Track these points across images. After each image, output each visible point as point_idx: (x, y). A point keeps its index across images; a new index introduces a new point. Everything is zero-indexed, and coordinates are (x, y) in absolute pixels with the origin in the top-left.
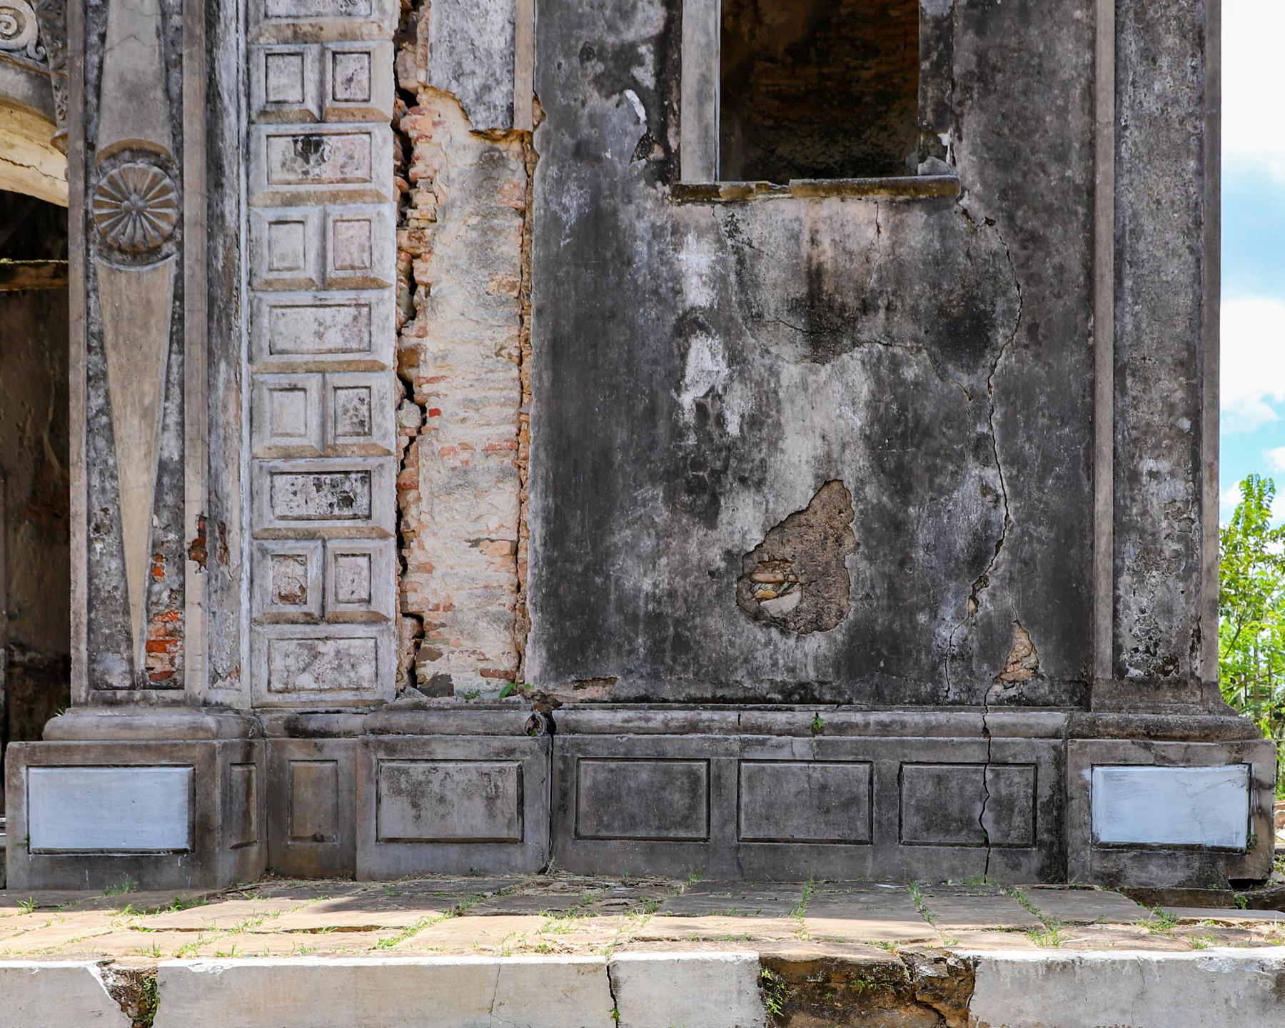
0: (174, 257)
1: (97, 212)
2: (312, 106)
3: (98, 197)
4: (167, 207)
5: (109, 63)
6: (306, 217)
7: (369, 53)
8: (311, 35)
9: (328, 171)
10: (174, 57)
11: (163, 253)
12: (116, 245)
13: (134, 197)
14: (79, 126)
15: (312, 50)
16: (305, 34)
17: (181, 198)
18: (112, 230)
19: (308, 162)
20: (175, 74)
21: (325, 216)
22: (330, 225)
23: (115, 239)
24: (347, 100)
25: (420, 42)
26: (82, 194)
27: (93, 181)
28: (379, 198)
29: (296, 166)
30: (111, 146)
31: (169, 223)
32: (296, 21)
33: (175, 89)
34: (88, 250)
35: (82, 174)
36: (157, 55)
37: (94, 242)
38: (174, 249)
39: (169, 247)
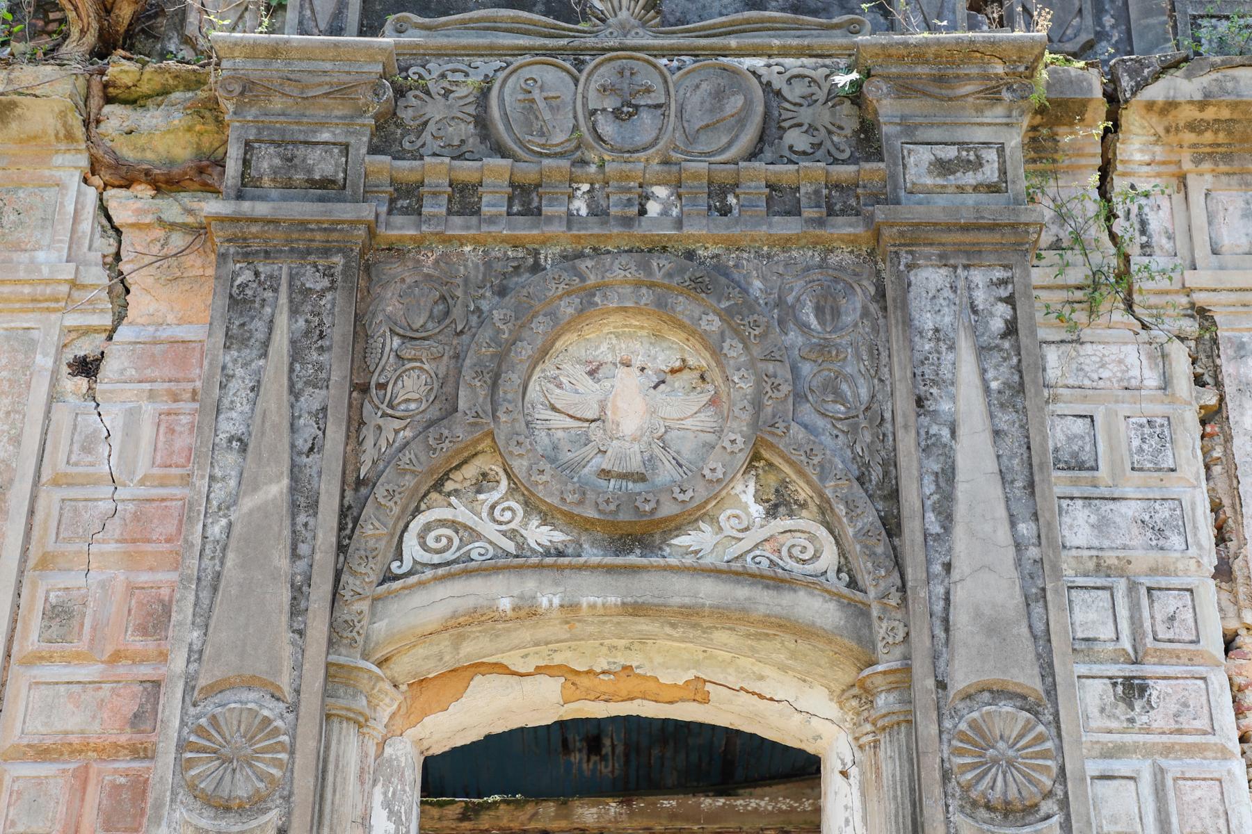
0: (1055, 819)
1: (960, 761)
2: (1126, 644)
3: (955, 743)
4: (1045, 758)
5: (958, 596)
6: (1138, 772)
7: (1191, 591)
8: (1116, 568)
9: (1158, 719)
10: (1034, 590)
11: (1042, 813)
12: (982, 802)
13: (1001, 745)
14: (928, 661)
15: (1121, 585)
16: (1109, 567)
17: (1060, 748)
18: (977, 783)
19: (1133, 710)
20: (1037, 609)
21: (1159, 773)
22: (1169, 782)
23: (984, 794)
24: (1170, 641)
25: (1240, 580)
26: (937, 739)
27: (948, 724)
28: (1224, 754)
29: (1118, 712)
30: (969, 686)
31: (1049, 776)
32: (1100, 554)
33: (1039, 627)
34: (947, 806)
35: (935, 716)
36: (1017, 588)
37: (953, 795)
38: (1056, 808)
39: (1048, 806)
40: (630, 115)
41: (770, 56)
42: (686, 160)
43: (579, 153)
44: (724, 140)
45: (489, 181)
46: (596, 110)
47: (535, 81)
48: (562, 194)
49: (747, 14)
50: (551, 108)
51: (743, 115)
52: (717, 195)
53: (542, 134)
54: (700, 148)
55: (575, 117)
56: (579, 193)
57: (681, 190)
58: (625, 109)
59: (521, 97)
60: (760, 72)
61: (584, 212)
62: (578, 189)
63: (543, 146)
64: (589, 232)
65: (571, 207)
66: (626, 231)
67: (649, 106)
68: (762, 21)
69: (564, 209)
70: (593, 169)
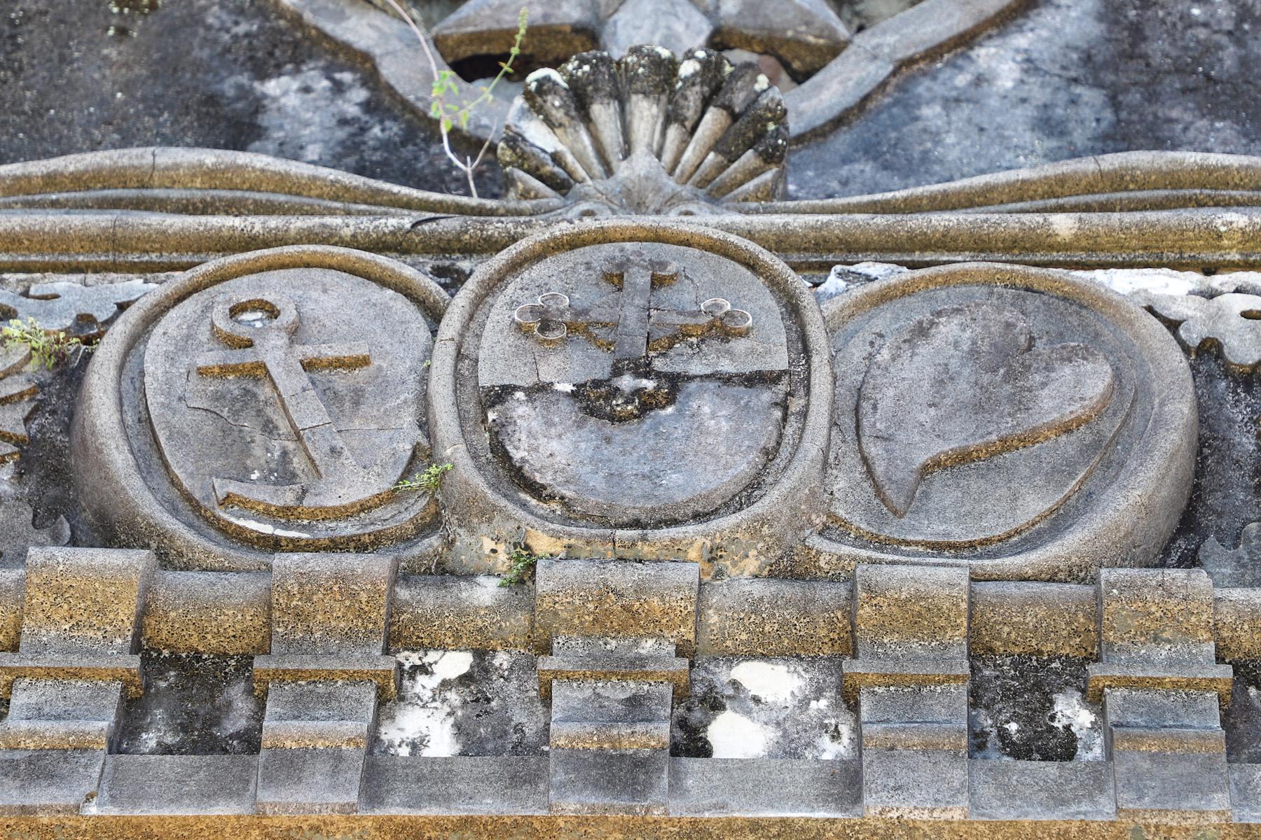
40: (647, 404)
41: (1209, 270)
42: (873, 562)
43: (434, 541)
44: (1034, 505)
45: (49, 634)
46: (508, 390)
47: (272, 312)
48: (354, 679)
49: (1112, 161)
50: (331, 397)
51: (1108, 428)
52: (1010, 695)
53: (285, 476)
54: (933, 530)
55: (425, 424)
56: (424, 685)
57: (853, 667)
58: (627, 382)
59: (211, 357)
60: (1173, 312)
61: (442, 744)
62: (424, 669)
63: (286, 515)
64: (458, 811)
65: (389, 733)
66: (616, 806)
67: (726, 380)
68: (1173, 179)
69: (357, 727)
70: (486, 592)
